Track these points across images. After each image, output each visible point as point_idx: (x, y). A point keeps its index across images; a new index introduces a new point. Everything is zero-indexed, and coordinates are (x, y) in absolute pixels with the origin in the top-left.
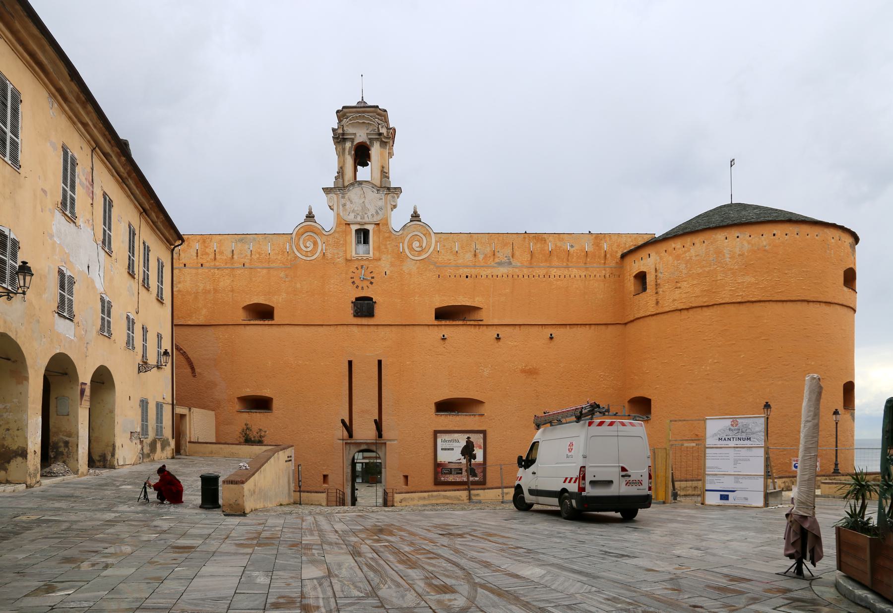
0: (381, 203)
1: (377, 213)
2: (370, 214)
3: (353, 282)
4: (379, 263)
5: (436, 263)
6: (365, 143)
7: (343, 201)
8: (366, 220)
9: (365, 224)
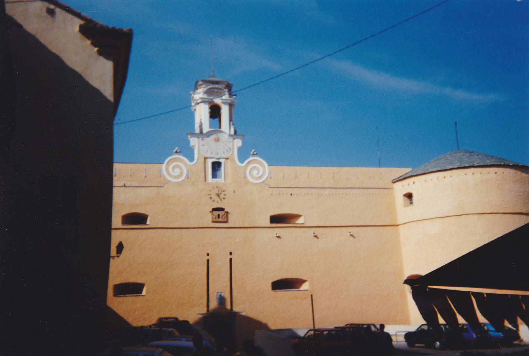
3: (211, 198)
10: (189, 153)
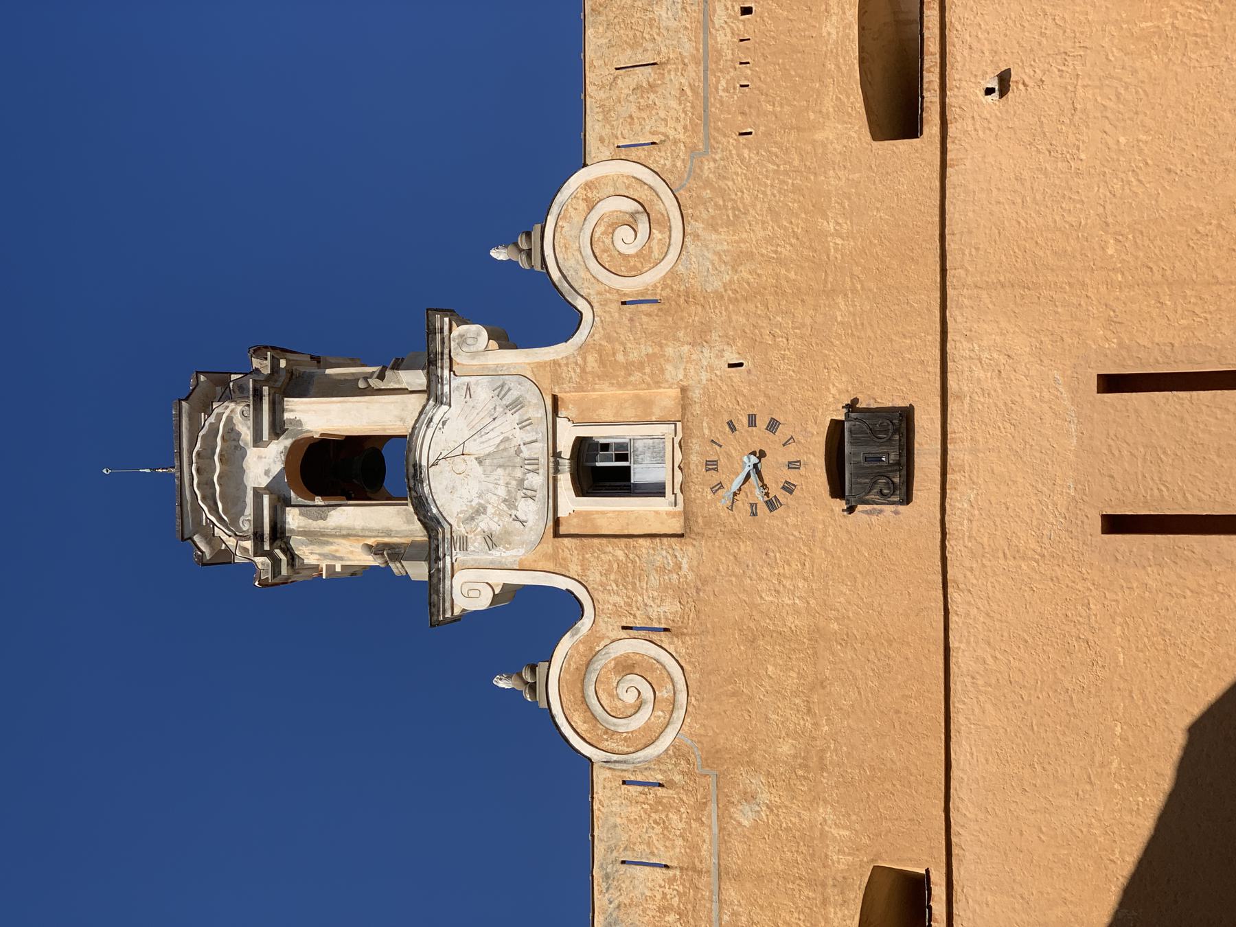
0: (483, 391)
1: (516, 405)
2: (520, 436)
4: (696, 394)
5: (693, 151)
6: (290, 453)
7: (476, 543)
8: (540, 450)
9: (556, 455)
10: (535, 617)
